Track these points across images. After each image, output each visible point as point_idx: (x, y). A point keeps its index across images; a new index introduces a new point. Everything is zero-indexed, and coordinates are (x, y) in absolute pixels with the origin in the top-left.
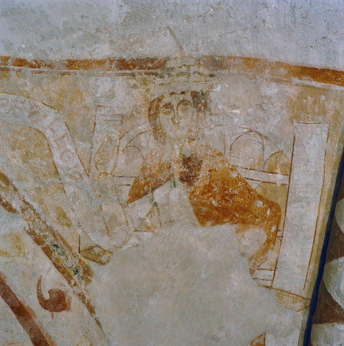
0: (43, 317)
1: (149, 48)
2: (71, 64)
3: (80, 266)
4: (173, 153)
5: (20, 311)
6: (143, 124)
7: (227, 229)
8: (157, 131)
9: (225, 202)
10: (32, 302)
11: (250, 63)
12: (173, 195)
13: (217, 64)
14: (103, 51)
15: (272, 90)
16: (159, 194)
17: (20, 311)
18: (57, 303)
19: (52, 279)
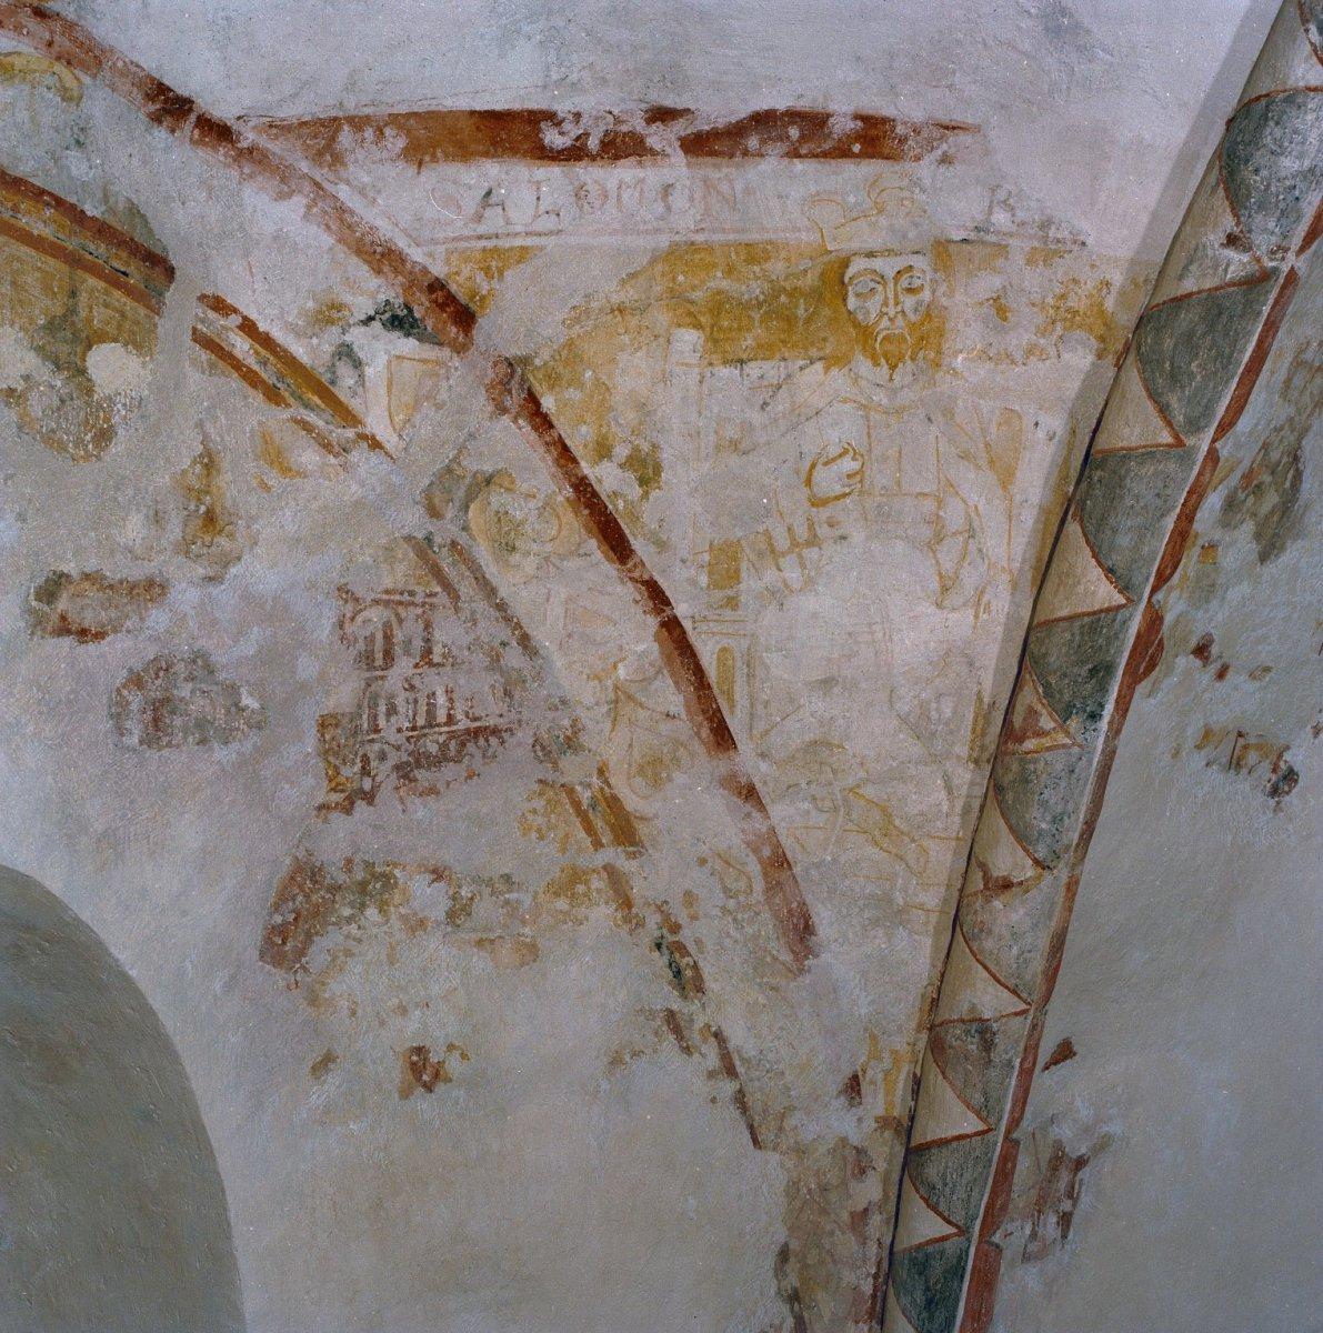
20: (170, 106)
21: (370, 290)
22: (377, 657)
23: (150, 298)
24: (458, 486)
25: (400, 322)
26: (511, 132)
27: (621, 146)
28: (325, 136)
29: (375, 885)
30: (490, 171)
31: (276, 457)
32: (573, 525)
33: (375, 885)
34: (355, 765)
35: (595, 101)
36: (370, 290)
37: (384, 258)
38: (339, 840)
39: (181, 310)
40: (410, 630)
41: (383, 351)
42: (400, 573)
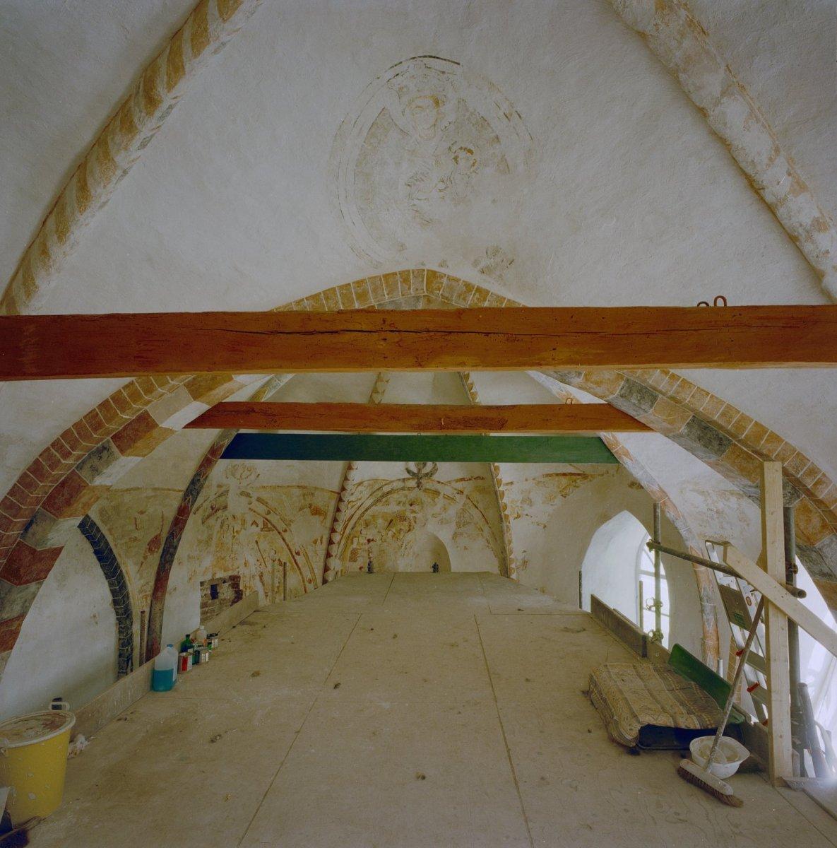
0: (283, 533)
1: (302, 484)
2: (288, 486)
3: (289, 523)
4: (307, 503)
5: (279, 533)
6: (302, 498)
7: (317, 516)
8: (304, 499)
9: (316, 512)
10: (281, 531)
11: (322, 489)
12: (307, 510)
13: (316, 488)
14: (294, 484)
15: (325, 494)
16: (304, 510)
17: (279, 533)
18: (285, 531)
19: (284, 526)
20: (439, 482)
21: (455, 492)
22: (460, 517)
23: (439, 495)
24: (465, 505)
25: (458, 493)
26: (462, 480)
27: (470, 479)
28: (450, 482)
29: (461, 534)
30: (461, 482)
31: (450, 504)
32: (474, 507)
33: (461, 534)
34: (459, 525)
35: (467, 477)
36: (455, 492)
37: (456, 489)
38: (460, 530)
39: (441, 495)
40: (462, 515)
41: (457, 495)
42: (461, 511)
